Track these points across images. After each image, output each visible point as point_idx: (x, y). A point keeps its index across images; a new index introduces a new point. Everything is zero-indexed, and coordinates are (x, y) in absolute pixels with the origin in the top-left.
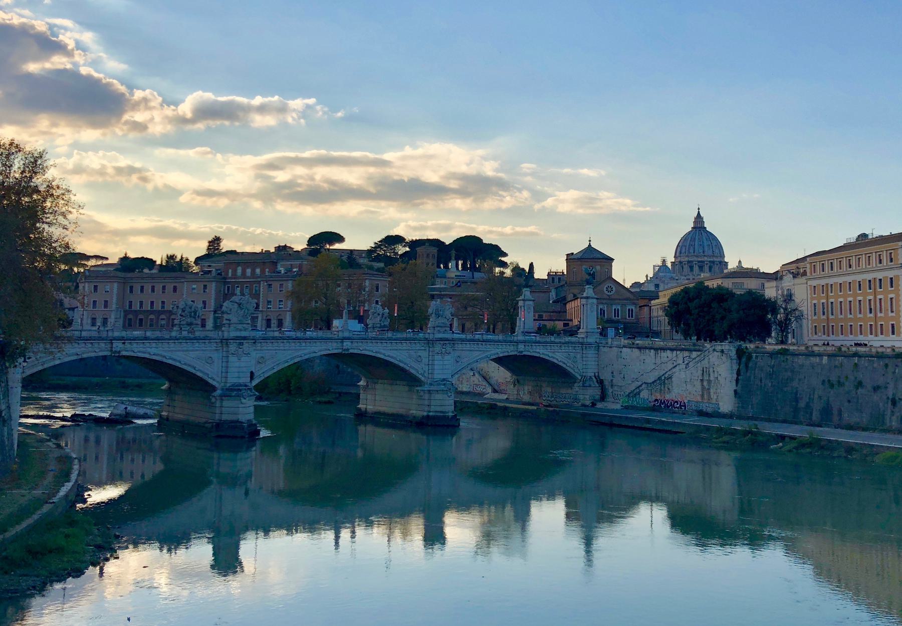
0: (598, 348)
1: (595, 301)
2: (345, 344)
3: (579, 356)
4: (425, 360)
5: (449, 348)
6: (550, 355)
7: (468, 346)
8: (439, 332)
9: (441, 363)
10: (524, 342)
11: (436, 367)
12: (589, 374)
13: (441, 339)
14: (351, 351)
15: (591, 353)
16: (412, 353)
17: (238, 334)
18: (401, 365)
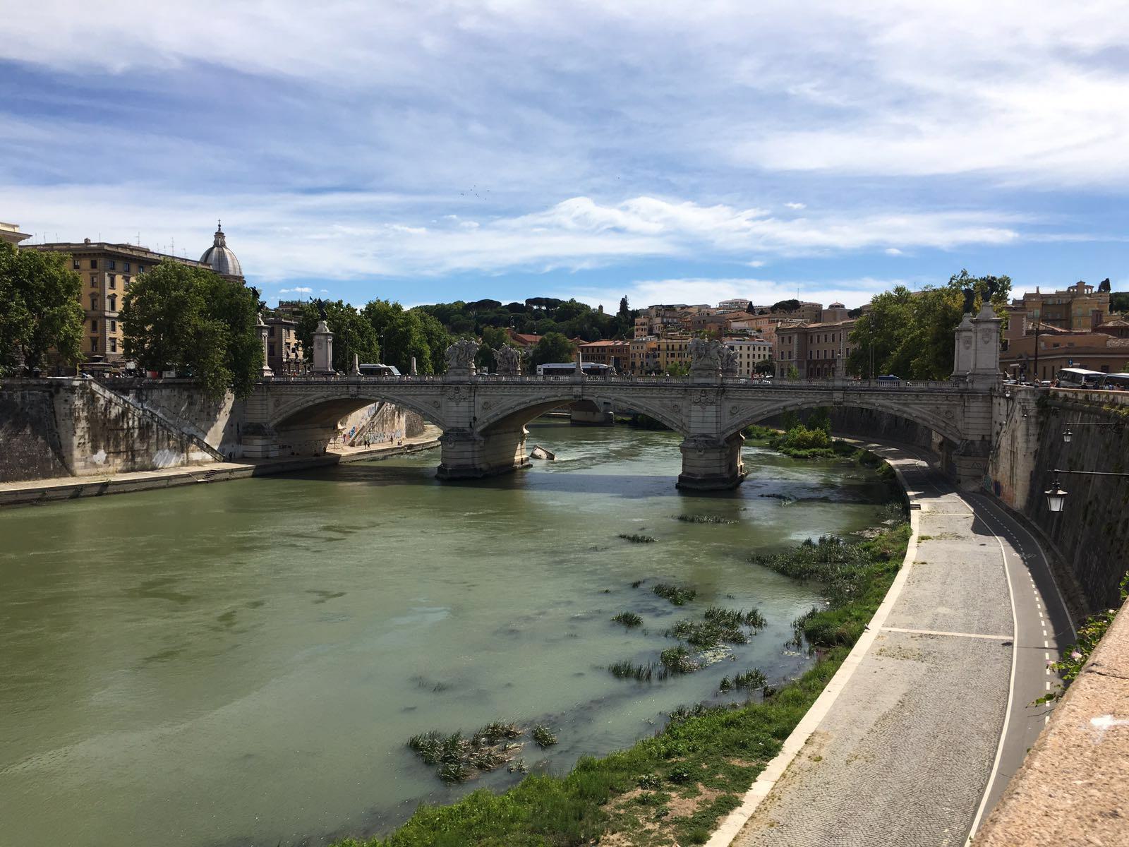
0: (990, 396)
1: (992, 326)
2: (575, 390)
3: (959, 410)
4: (684, 411)
5: (712, 396)
6: (896, 407)
7: (750, 395)
8: (700, 376)
9: (701, 414)
10: (844, 389)
11: (693, 419)
12: (970, 438)
13: (699, 385)
14: (585, 398)
15: (976, 407)
16: (666, 401)
17: (456, 378)
18: (650, 415)
